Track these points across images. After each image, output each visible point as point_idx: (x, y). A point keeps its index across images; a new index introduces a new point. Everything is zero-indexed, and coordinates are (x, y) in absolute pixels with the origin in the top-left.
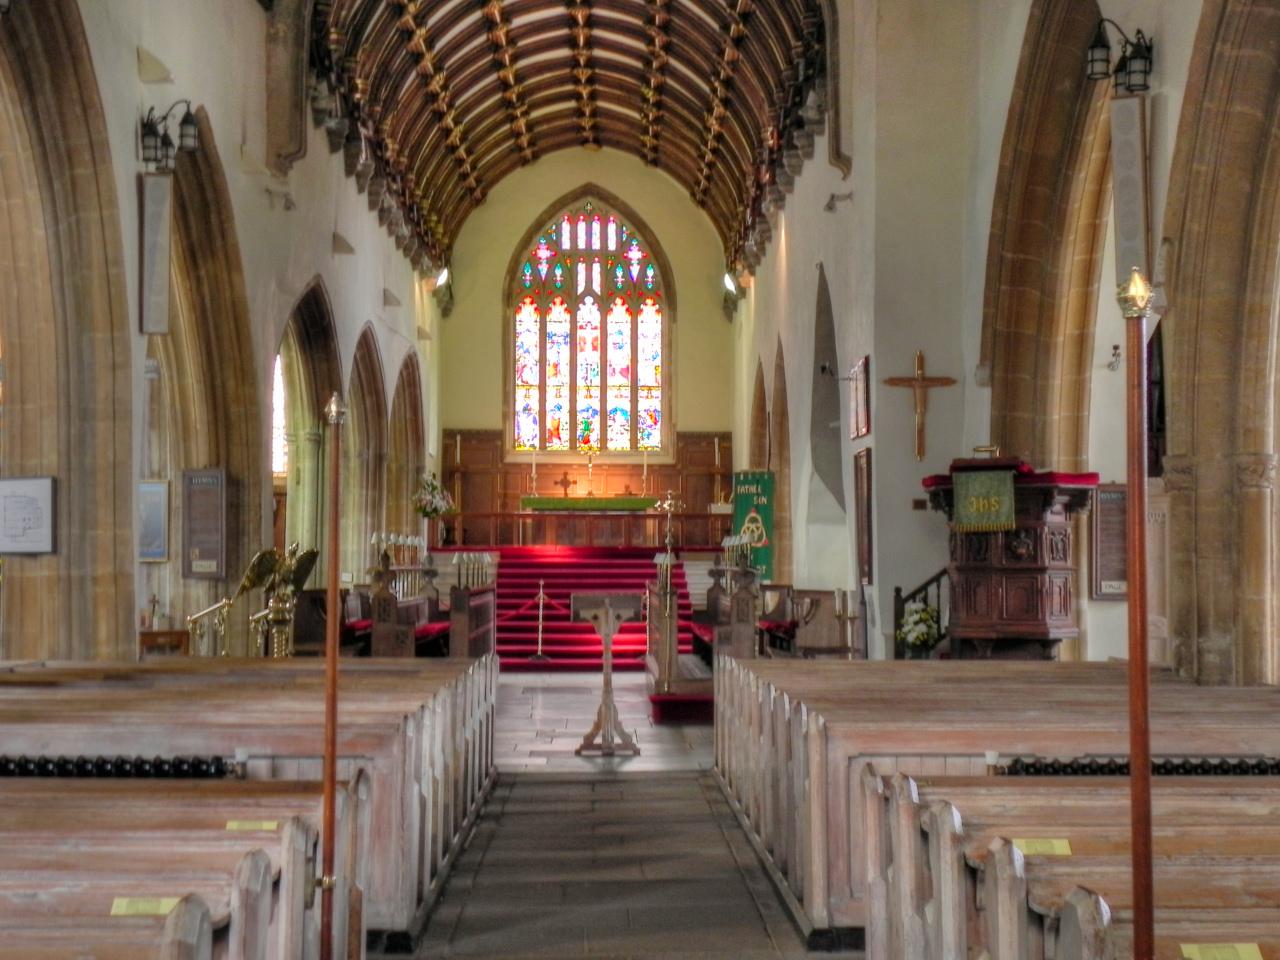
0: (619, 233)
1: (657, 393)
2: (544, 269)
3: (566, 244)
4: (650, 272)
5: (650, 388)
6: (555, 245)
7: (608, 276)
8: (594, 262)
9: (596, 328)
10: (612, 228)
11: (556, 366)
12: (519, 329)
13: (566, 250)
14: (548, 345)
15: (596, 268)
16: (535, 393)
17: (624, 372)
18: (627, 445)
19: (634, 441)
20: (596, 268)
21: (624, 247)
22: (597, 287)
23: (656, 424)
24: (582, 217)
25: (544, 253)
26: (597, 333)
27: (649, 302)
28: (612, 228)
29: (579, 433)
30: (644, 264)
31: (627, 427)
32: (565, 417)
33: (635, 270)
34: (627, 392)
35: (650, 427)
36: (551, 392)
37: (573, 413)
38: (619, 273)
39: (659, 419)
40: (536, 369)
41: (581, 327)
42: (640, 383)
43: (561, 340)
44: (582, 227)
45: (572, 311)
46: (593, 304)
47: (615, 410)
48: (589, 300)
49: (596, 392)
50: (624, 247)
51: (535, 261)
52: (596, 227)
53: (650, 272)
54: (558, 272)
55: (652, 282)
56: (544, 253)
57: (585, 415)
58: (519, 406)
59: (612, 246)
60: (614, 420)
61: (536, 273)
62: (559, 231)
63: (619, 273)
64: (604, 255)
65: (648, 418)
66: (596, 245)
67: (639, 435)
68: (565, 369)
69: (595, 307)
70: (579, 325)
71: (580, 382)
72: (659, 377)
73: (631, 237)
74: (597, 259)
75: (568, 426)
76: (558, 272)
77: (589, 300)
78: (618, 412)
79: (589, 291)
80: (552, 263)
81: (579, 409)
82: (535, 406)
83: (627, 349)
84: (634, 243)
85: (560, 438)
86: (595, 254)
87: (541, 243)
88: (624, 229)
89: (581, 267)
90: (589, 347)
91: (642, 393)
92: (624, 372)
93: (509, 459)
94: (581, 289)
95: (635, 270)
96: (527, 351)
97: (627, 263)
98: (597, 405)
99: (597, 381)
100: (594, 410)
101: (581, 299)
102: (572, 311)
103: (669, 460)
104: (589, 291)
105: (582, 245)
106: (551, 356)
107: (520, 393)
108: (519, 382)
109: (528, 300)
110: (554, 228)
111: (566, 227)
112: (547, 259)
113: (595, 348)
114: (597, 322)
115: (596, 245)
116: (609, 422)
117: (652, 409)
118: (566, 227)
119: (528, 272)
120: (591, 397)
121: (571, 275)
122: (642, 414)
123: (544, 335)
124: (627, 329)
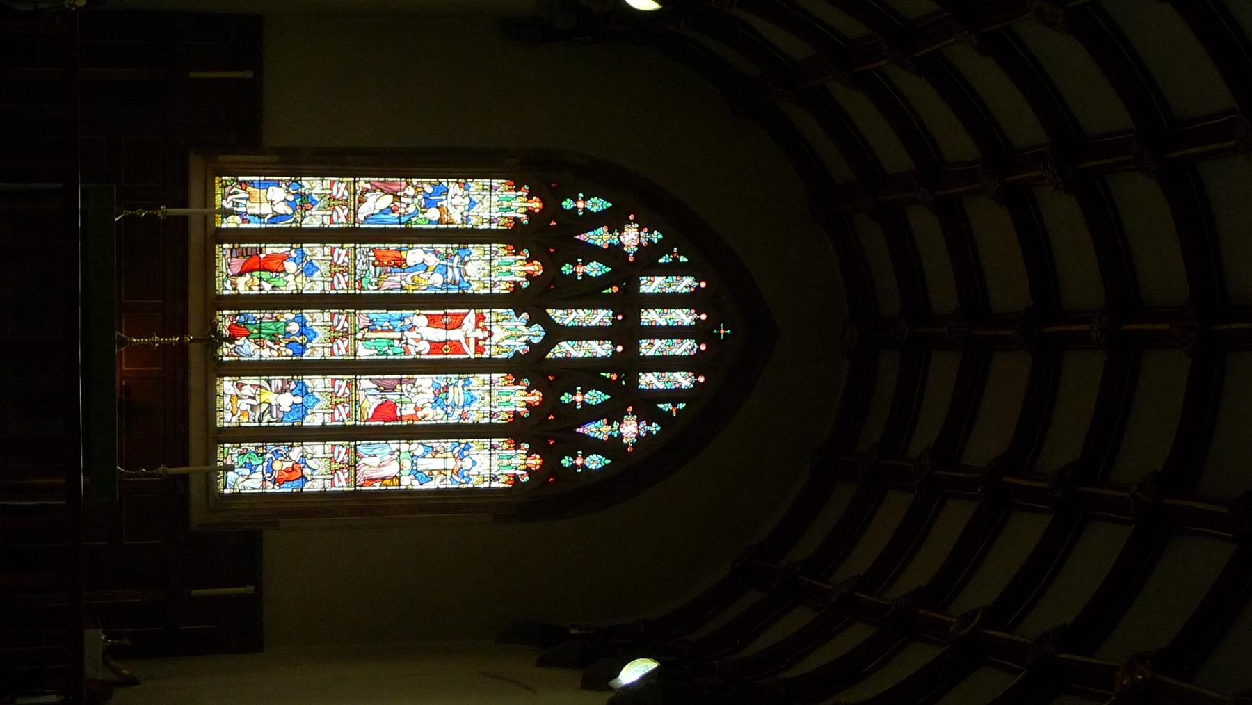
0: (673, 395)
1: (341, 483)
2: (599, 237)
3: (651, 285)
4: (595, 462)
5: (353, 466)
6: (647, 261)
7: (586, 372)
8: (615, 345)
9: (480, 349)
10: (683, 380)
11: (400, 264)
12: (475, 185)
13: (638, 285)
14: (441, 248)
15: (601, 349)
16: (341, 219)
17: (387, 409)
18: (227, 419)
19: (239, 435)
20: (601, 349)
21: (646, 405)
22: (565, 349)
23: (275, 481)
24: (703, 317)
25: (631, 237)
26: (471, 353)
27: (535, 461)
28: (683, 380)
29: (256, 314)
30: (612, 447)
31: (267, 418)
32: (289, 283)
33: (597, 430)
34: (342, 416)
35: (270, 469)
36: (342, 253)
37: (299, 301)
38: (595, 397)
39: (287, 488)
40: (391, 222)
41: (480, 318)
42: (362, 449)
43: (453, 274)
44: (684, 317)
45: (516, 300)
46: (528, 342)
47: (305, 392)
48: (537, 333)
49: (341, 351)
50: (646, 405)
51: (614, 222)
52: (685, 347)
53: (595, 462)
54: (595, 269)
55: (575, 466)
56: (631, 237)
57: (294, 327)
58: (314, 185)
59: (649, 380)
60: (283, 391)
61: (592, 221)
62: (674, 270)
63: (595, 397)
64: (631, 364)
65: (288, 464)
66: (650, 348)
67: (251, 446)
68: (393, 283)
69: (522, 347)
70: (486, 312)
71: (364, 317)
72: (377, 486)
73: (662, 418)
74: (620, 349)
75: (267, 288)
76: (595, 269)
77: (537, 333)
78: (298, 400)
79: (556, 333)
80: (613, 254)
81: (307, 314)
82: (314, 219)
83: (433, 416)
84: (655, 428)
85: (241, 274)
86: (632, 347)
87: (650, 232)
88: (681, 406)
89: (602, 317)
90: (439, 335)
91: (341, 450)
92: (387, 409)
93: (195, 164)
94: (557, 315)
95: (597, 430)
96: (429, 203)
97: (612, 413)
98: (316, 352)
99: (364, 353)
100: (303, 346)
101: (539, 317)
102: (516, 300)
103: (197, 515)
104: (556, 333)
105: (651, 317)
106: (416, 255)
107: (340, 187)
108: (363, 183)
109: (536, 205)
110: (683, 259)
111: (685, 284)
112: (621, 245)
113: (436, 346)
114: (492, 352)
115: (650, 348)
116: (277, 381)
117: (307, 471)
118: (685, 284)
119: (597, 204)
120: (333, 340)
121: (587, 294)
122: (296, 454)
123: (465, 237)
124: (477, 415)
